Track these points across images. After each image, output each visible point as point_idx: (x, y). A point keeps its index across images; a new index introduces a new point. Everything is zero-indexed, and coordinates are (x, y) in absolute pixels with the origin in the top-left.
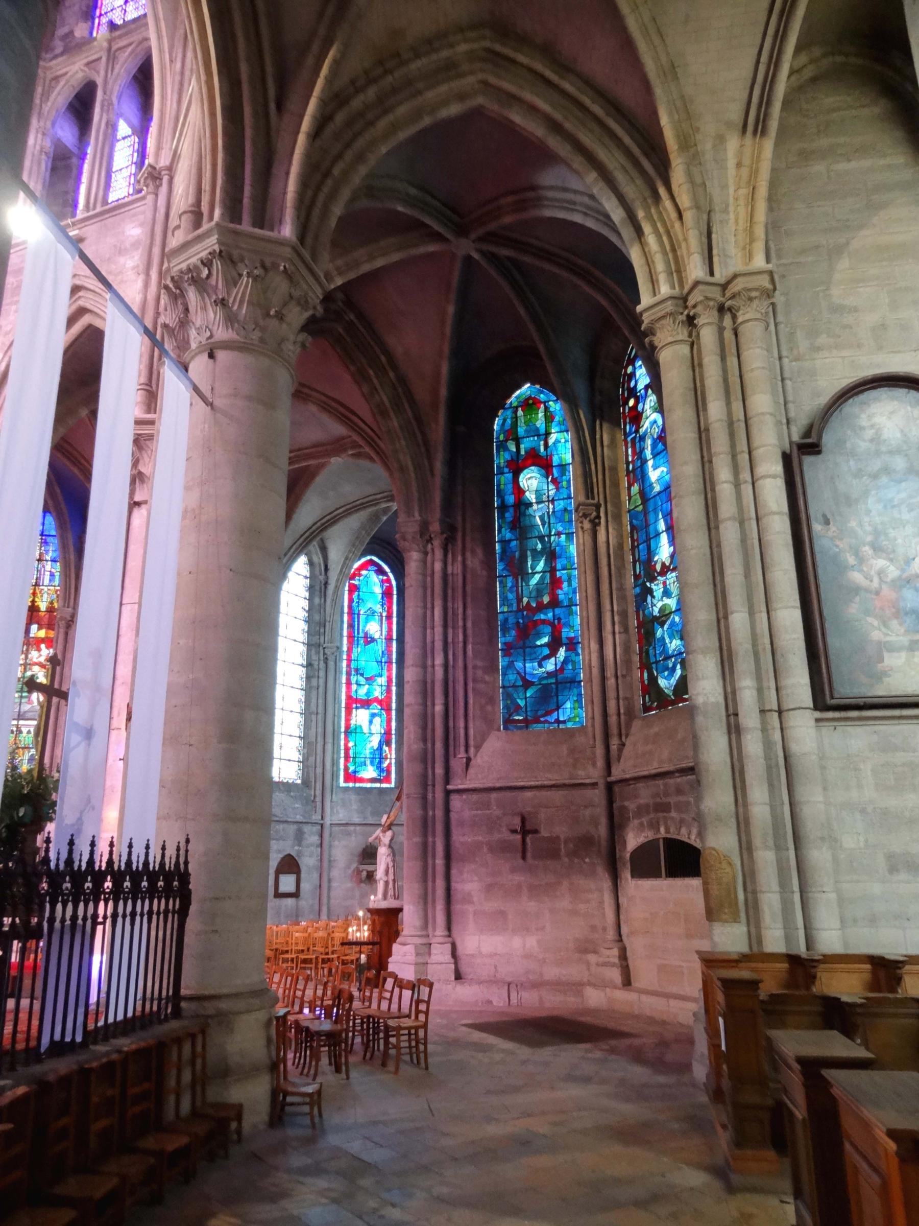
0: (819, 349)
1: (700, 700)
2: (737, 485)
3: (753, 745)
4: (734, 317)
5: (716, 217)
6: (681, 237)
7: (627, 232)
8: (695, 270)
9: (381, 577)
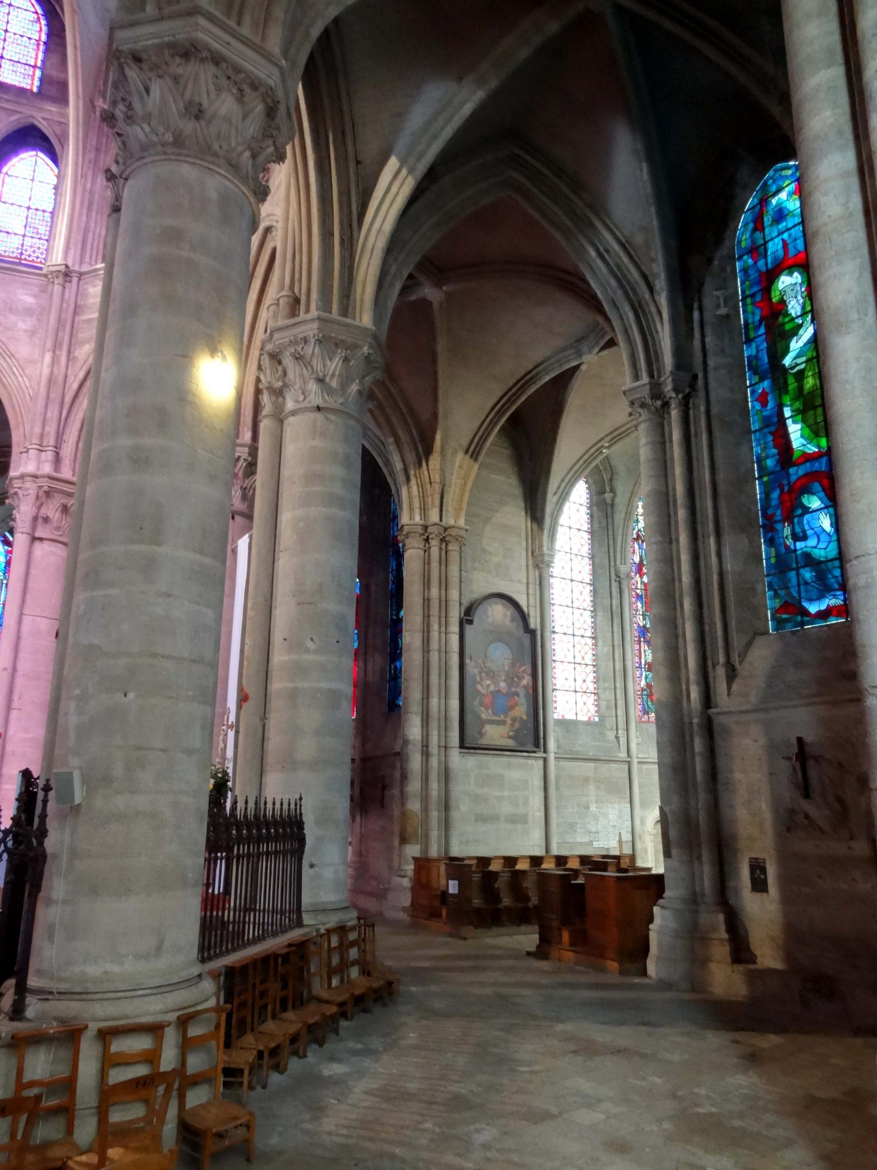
0: (475, 569)
1: (411, 738)
2: (440, 633)
3: (434, 762)
4: (447, 545)
5: (446, 489)
6: (429, 493)
7: (401, 478)
8: (434, 517)
9: (6, 548)
